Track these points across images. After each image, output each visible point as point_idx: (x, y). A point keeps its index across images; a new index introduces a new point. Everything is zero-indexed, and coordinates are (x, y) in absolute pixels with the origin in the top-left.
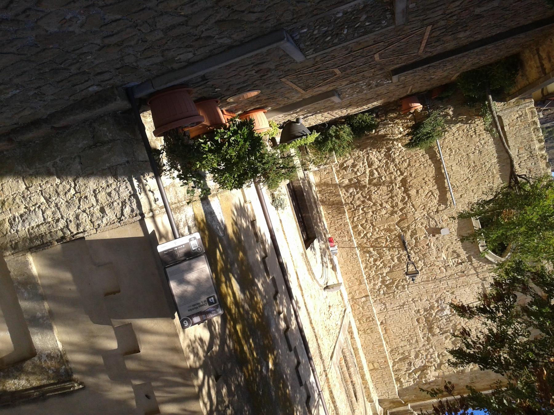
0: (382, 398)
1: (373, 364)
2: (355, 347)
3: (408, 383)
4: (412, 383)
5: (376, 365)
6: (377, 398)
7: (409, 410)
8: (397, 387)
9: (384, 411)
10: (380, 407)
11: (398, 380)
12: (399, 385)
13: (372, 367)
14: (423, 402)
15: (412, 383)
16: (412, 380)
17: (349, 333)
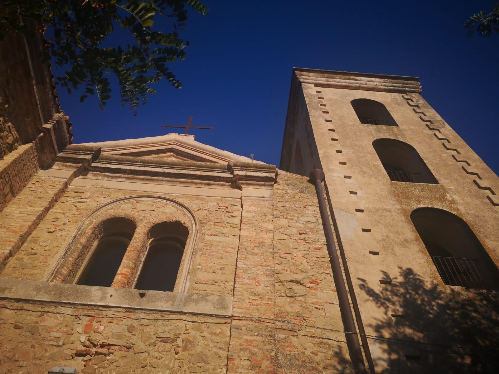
0: (37, 165)
1: (6, 196)
2: (20, 244)
3: (12, 130)
4: (10, 124)
5: (7, 190)
6: (41, 172)
7: (54, 126)
8: (22, 148)
9: (61, 161)
10: (55, 167)
11: (11, 148)
12: (16, 144)
13: (10, 195)
14: (39, 106)
15: (10, 124)
16: (7, 125)
17: (5, 265)
